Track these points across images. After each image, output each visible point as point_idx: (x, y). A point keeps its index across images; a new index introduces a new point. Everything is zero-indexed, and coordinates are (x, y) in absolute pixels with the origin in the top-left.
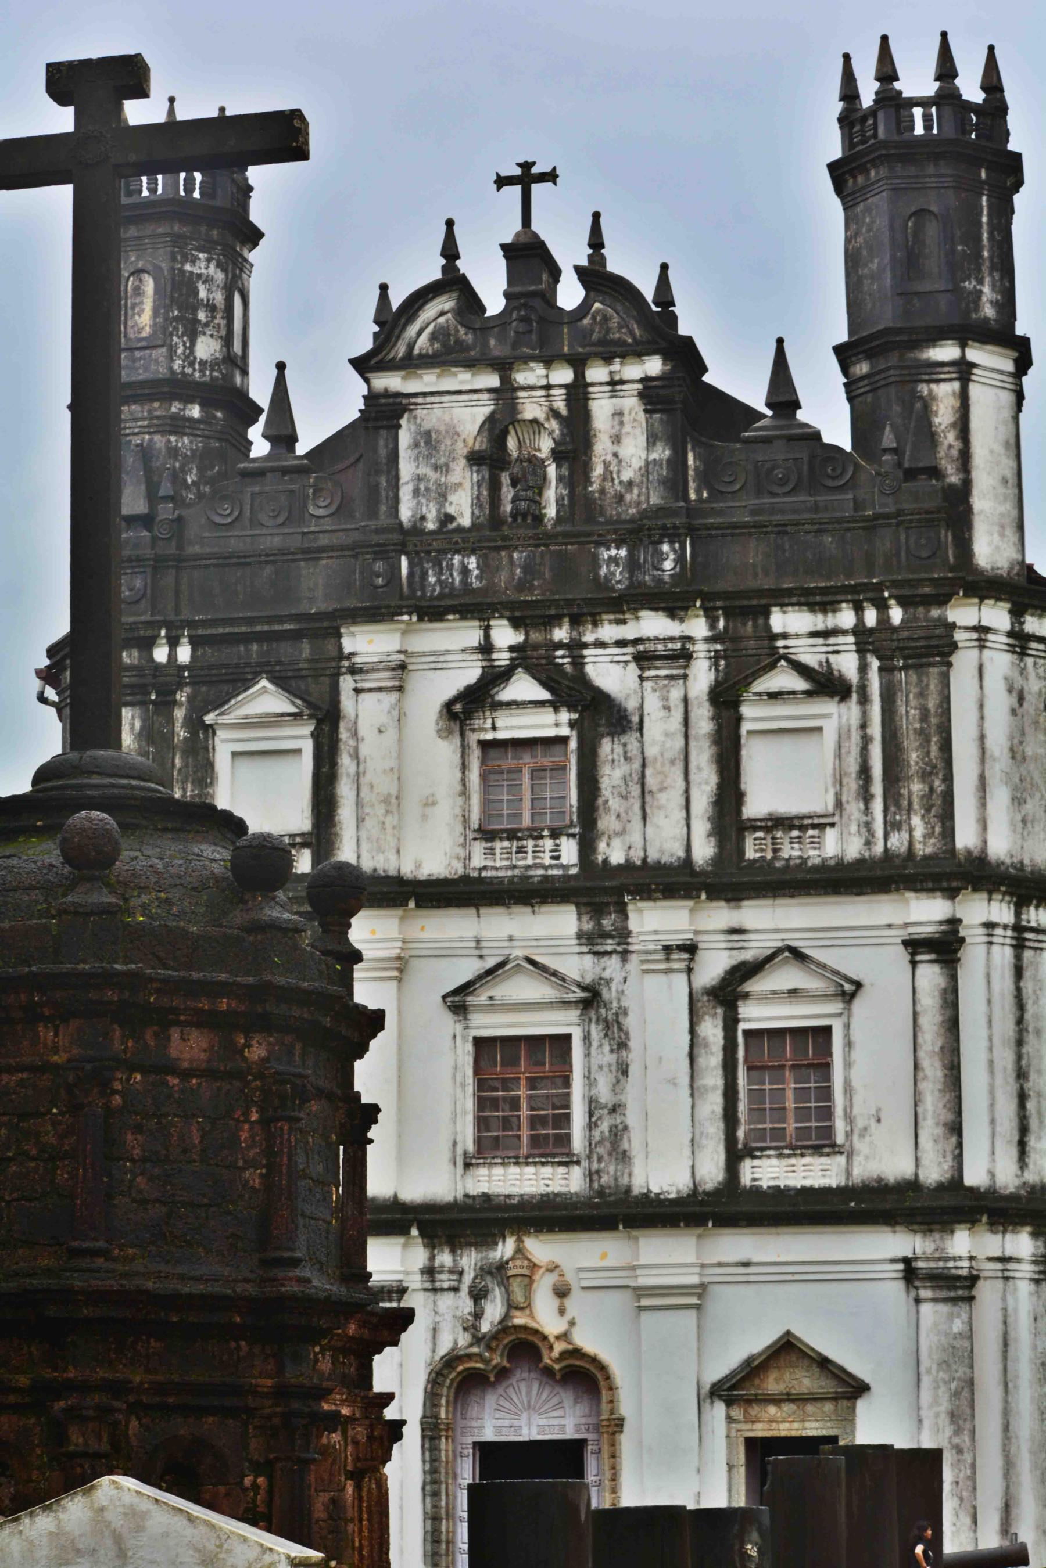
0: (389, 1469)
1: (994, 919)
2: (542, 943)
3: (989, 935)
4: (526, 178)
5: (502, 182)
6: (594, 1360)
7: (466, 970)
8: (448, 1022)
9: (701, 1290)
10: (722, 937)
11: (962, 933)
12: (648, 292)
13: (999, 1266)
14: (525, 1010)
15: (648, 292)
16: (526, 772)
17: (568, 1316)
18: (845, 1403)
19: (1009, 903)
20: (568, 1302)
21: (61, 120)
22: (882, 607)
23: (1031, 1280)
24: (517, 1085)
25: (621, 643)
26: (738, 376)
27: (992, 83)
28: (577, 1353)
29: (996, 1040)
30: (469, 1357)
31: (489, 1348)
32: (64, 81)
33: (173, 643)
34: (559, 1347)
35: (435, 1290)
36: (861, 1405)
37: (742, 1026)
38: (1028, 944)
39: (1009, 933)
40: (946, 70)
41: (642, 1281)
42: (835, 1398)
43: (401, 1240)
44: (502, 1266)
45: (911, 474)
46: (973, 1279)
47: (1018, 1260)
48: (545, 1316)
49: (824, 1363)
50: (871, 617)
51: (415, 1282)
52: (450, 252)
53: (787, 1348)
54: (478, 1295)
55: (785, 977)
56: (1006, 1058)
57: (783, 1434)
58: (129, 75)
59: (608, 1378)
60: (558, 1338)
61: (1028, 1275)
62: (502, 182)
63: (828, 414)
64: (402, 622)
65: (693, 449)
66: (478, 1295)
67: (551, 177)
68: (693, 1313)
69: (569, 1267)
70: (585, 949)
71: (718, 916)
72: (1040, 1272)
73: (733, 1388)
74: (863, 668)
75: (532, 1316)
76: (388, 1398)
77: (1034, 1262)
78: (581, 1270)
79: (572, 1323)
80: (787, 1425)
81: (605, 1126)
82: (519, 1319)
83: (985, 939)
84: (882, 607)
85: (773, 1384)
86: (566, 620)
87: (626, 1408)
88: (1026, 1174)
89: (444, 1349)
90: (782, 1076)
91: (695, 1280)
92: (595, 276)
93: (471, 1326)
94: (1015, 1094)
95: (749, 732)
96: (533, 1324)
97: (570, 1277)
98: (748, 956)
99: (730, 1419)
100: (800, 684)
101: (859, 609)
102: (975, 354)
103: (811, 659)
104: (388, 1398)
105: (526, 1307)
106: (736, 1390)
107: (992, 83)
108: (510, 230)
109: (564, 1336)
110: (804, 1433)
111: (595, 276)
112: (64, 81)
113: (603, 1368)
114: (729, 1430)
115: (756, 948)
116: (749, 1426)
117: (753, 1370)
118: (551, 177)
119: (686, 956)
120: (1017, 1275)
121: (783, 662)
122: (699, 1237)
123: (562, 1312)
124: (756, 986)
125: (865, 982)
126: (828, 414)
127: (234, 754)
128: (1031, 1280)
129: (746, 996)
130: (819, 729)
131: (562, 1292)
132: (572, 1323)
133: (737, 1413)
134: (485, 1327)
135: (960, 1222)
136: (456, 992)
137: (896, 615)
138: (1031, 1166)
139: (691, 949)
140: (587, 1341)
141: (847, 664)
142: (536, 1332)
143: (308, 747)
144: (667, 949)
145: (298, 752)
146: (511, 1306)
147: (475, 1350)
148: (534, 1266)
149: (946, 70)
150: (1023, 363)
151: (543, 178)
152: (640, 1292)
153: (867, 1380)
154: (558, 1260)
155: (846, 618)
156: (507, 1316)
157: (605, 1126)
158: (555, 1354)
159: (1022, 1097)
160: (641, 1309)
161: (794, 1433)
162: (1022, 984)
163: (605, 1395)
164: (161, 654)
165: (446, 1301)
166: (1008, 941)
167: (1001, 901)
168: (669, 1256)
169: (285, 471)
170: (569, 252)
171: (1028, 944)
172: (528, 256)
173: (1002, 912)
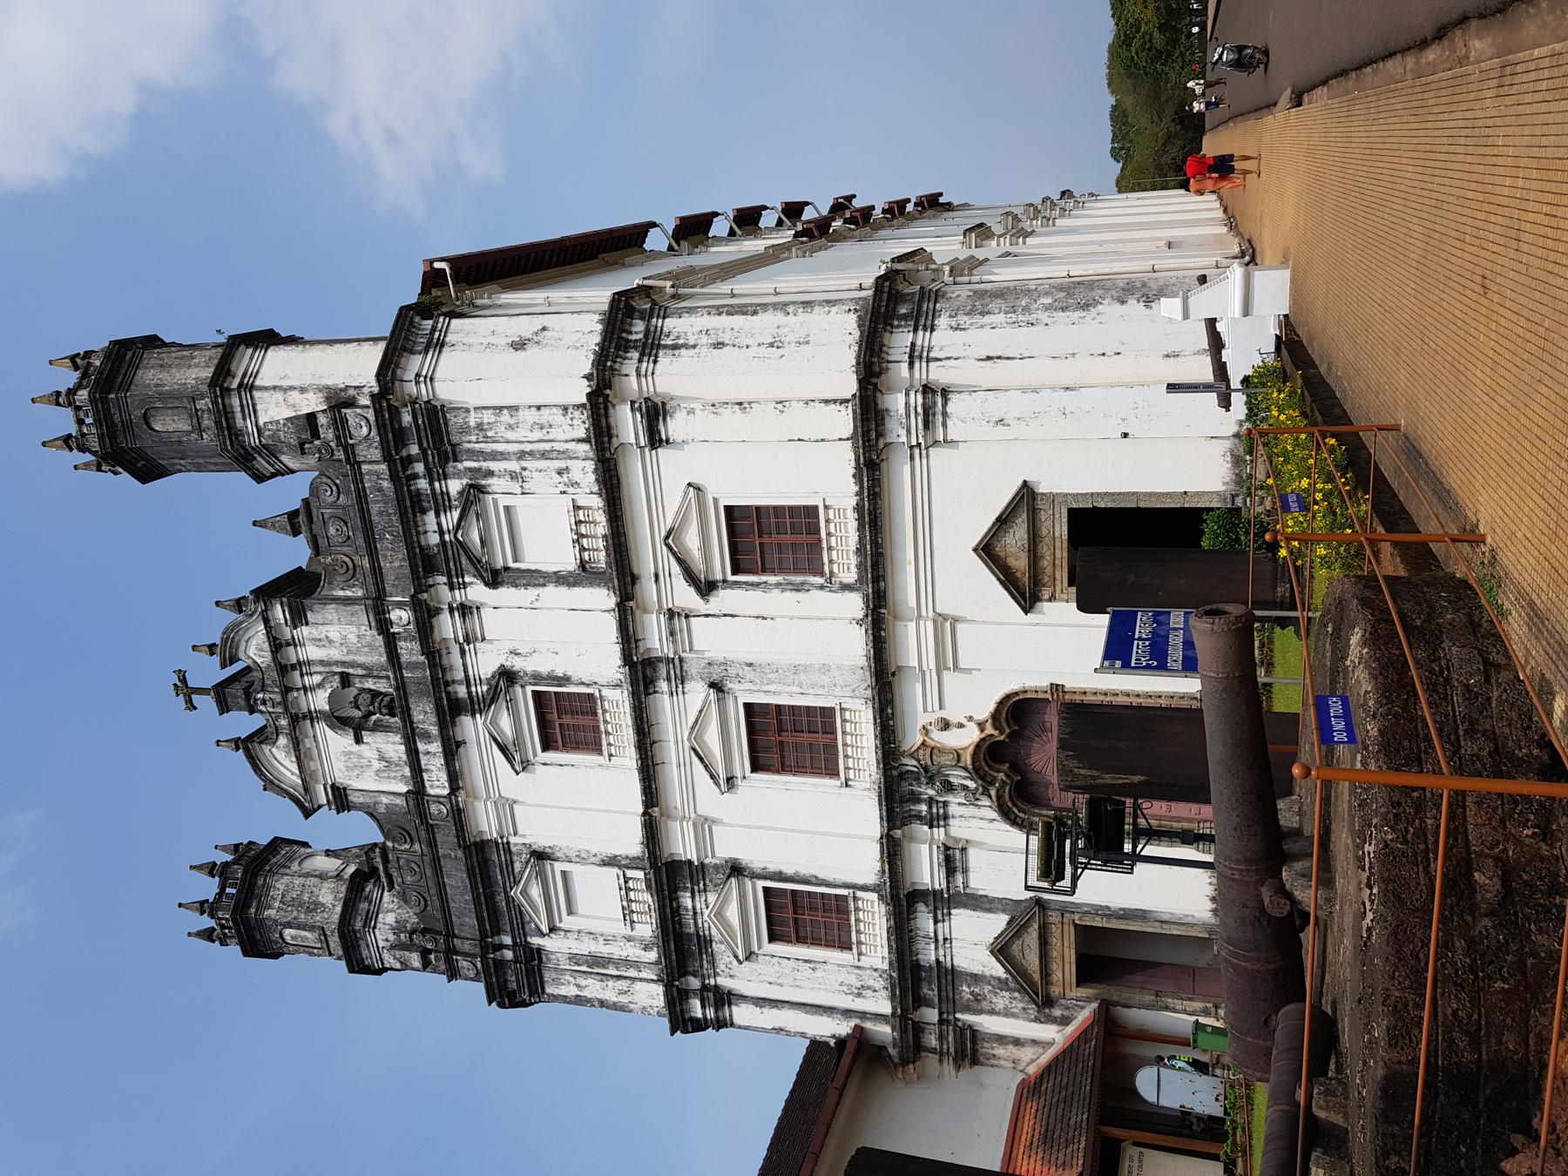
6: (1001, 703)
8: (743, 788)
14: (727, 739)
16: (567, 720)
17: (965, 722)
18: (1040, 504)
20: (953, 719)
24: (785, 739)
25: (463, 652)
28: (995, 716)
30: (999, 797)
31: (992, 783)
33: (502, 947)
34: (990, 730)
35: (946, 817)
36: (1042, 489)
37: (731, 578)
41: (933, 666)
42: (1033, 513)
43: (905, 843)
46: (927, 389)
47: (913, 345)
48: (966, 738)
49: (1003, 522)
51: (939, 834)
53: (987, 550)
54: (949, 787)
55: (692, 540)
57: (1065, 555)
59: (1017, 694)
60: (982, 731)
65: (332, 589)
66: (949, 787)
68: (959, 626)
71: (648, 589)
73: (1023, 596)
74: (458, 475)
75: (965, 749)
78: (925, 710)
79: (970, 719)
80: (1058, 552)
82: (967, 759)
84: (410, 460)
85: (1020, 563)
86: (450, 689)
87: (1044, 683)
89: (995, 815)
90: (767, 541)
91: (930, 625)
93: (972, 798)
95: (516, 560)
96: (971, 749)
97: (933, 718)
99: (1052, 598)
101: (416, 476)
103: (456, 514)
106: (1027, 595)
109: (981, 726)
110: (1065, 537)
113: (1008, 697)
114: (1061, 600)
116: (1058, 583)
117: (1008, 579)
122: (895, 617)
123: (961, 726)
124: (698, 565)
127: (570, 913)
130: (507, 508)
131: (946, 725)
132: (970, 719)
133: (1046, 594)
135: (876, 404)
136: (717, 784)
139: (671, 614)
140: (985, 710)
141: (454, 486)
142: (978, 746)
143: (559, 867)
144: (672, 633)
145: (564, 873)
147: (993, 793)
148: (923, 744)
151: (184, 681)
153: (1020, 483)
154: (919, 726)
156: (965, 769)
158: (996, 733)
160: (956, 667)
161: (1065, 545)
163: (1029, 696)
164: (509, 955)
165: (953, 809)
168: (914, 644)
172: (223, 695)
173: (630, 365)
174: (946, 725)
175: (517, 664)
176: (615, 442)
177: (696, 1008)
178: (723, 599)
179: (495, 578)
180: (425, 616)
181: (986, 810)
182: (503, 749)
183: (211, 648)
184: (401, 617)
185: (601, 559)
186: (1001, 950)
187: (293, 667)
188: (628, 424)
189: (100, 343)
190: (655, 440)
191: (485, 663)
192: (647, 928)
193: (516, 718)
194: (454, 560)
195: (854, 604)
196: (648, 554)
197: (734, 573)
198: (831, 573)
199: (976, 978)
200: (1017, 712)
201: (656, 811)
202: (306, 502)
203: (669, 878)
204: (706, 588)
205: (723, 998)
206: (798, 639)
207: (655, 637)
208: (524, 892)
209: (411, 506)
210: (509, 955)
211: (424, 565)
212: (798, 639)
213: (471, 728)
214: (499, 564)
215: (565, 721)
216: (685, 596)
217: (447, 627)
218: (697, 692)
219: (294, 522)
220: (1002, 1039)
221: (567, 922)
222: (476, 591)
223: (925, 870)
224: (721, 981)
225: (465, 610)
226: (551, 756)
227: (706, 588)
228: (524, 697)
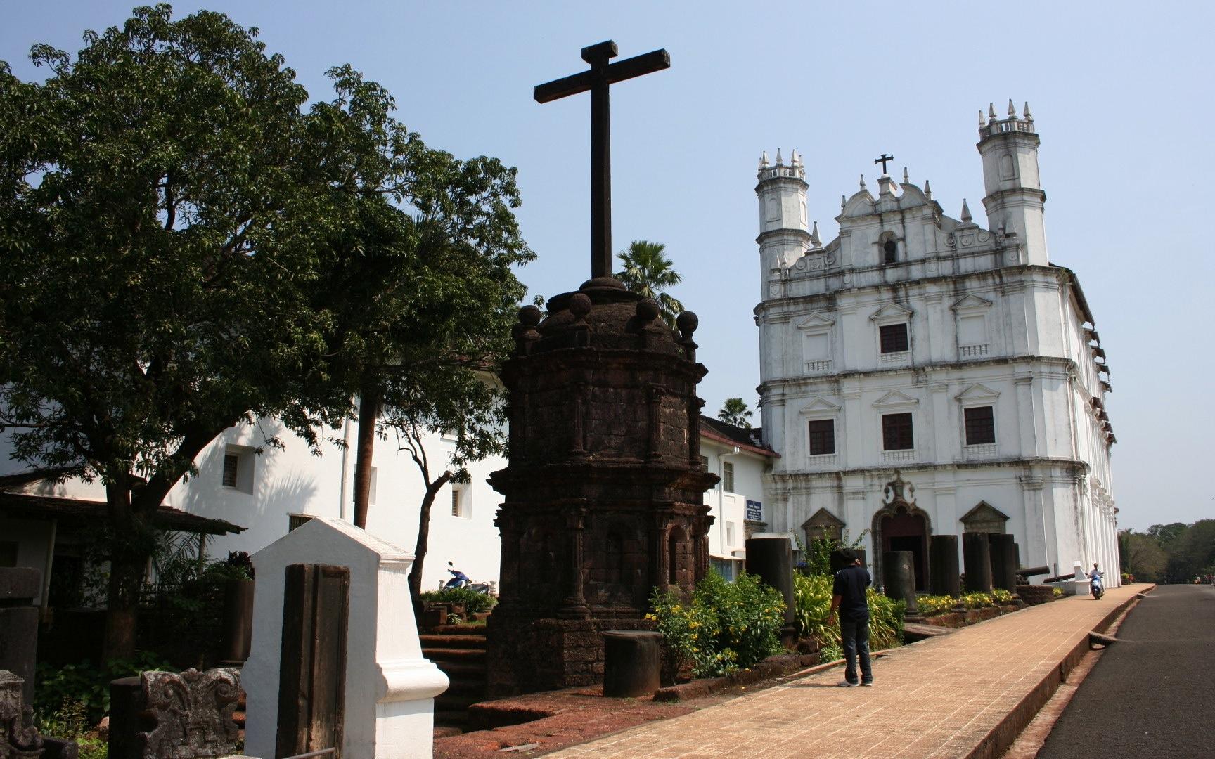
0: (709, 535)
4: (884, 159)
5: (877, 161)
7: (879, 395)
9: (954, 489)
12: (923, 189)
15: (923, 189)
21: (586, 67)
22: (1001, 277)
26: (952, 212)
27: (1027, 115)
28: (917, 509)
32: (588, 54)
40: (1012, 111)
44: (892, 484)
45: (1007, 236)
48: (908, 498)
49: (995, 511)
50: (997, 280)
52: (862, 185)
53: (983, 506)
58: (607, 49)
62: (877, 161)
63: (981, 219)
66: (887, 491)
67: (891, 158)
69: (913, 482)
71: (955, 374)
76: (708, 508)
85: (979, 516)
92: (905, 185)
98: (965, 387)
100: (976, 303)
102: (1025, 198)
104: (708, 508)
105: (902, 495)
107: (1027, 115)
108: (880, 175)
109: (914, 504)
111: (905, 185)
112: (588, 54)
115: (968, 383)
118: (891, 158)
126: (981, 219)
131: (912, 490)
134: (889, 501)
140: (920, 505)
141: (991, 296)
142: (906, 504)
146: (896, 495)
149: (1012, 111)
150: (1043, 198)
152: (935, 491)
155: (990, 281)
156: (895, 499)
169: (819, 252)
170: (898, 179)
172: (884, 181)
174: (912, 490)
175: (917, 320)
177: (775, 393)
178: (955, 406)
179: (954, 309)
180: (934, 280)
181: (880, 506)
182: (879, 312)
183: (906, 177)
184: (933, 269)
185: (965, 357)
186: (823, 512)
188: (1022, 370)
189: (1037, 128)
190: (1017, 381)
191: (916, 303)
192: (806, 371)
193: (894, 317)
194: (959, 295)
195: (959, 459)
196: (970, 375)
199: (808, 502)
200: (920, 518)
202: (977, 227)
203: (836, 380)
204: (958, 399)
205: (783, 403)
206: (939, 434)
207: (939, 377)
208: (816, 317)
209: (981, 275)
210: (785, 309)
211: (959, 279)
212: (939, 434)
213: (887, 295)
215: (894, 339)
216: (955, 390)
217: (932, 289)
218: (914, 393)
219: (967, 217)
220: (785, 513)
221: (804, 336)
222: (948, 302)
223: (851, 484)
224: (788, 403)
225: (940, 297)
227: (958, 399)
228: (903, 320)
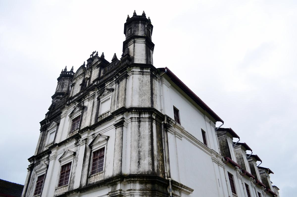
1: (135, 117)
2: (72, 148)
3: (131, 120)
10: (92, 136)
11: (125, 120)
13: (129, 192)
19: (137, 114)
23: (139, 195)
29: (132, 141)
33: (48, 122)
38: (141, 121)
39: (136, 119)
47: (135, 190)
56: (135, 144)
61: (138, 194)
64: (66, 107)
70: (75, 146)
72: (142, 193)
77: (140, 190)
81: (72, 177)
83: (131, 121)
84: (118, 75)
88: (140, 169)
94: (137, 151)
119: (85, 141)
120: (135, 194)
121: (106, 90)
125: (110, 136)
128: (139, 195)
129: (93, 146)
136: (60, 159)
137: (120, 74)
138: (141, 167)
141: (114, 87)
157: (72, 177)
159: (139, 152)
162: (140, 129)
166: (136, 121)
167: (135, 114)
171: (141, 121)
176: (116, 116)
187: (92, 69)
197: (94, 152)
198: (92, 177)
201: (57, 146)
214: (101, 100)
226: (72, 121)
